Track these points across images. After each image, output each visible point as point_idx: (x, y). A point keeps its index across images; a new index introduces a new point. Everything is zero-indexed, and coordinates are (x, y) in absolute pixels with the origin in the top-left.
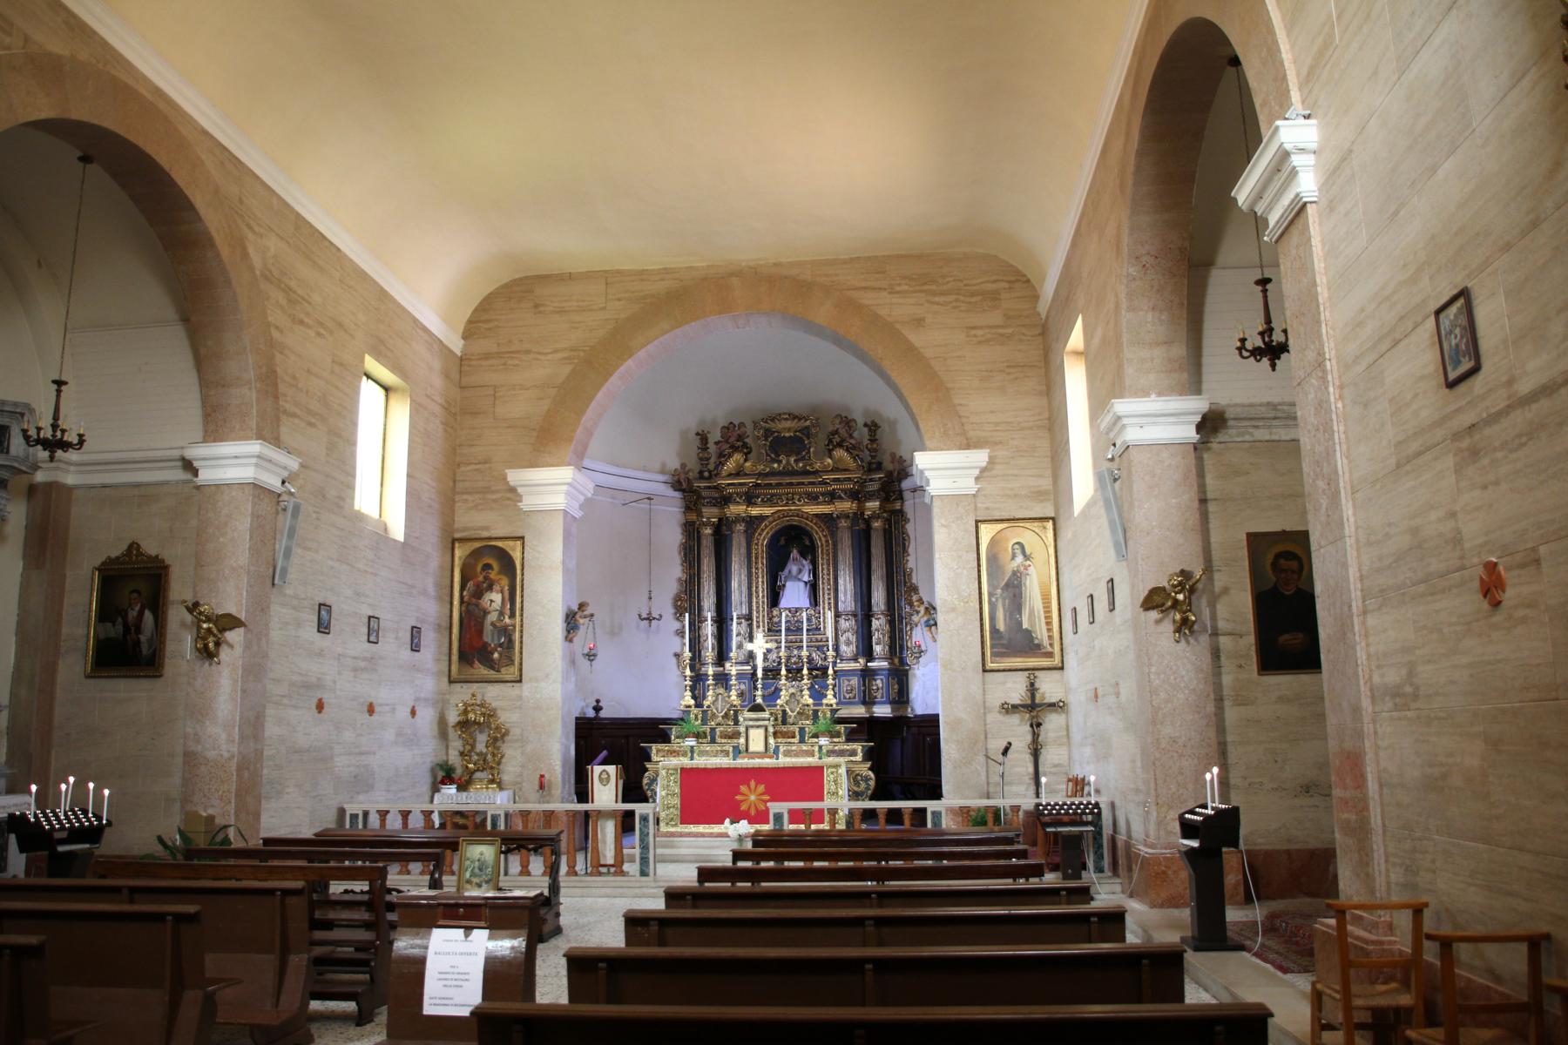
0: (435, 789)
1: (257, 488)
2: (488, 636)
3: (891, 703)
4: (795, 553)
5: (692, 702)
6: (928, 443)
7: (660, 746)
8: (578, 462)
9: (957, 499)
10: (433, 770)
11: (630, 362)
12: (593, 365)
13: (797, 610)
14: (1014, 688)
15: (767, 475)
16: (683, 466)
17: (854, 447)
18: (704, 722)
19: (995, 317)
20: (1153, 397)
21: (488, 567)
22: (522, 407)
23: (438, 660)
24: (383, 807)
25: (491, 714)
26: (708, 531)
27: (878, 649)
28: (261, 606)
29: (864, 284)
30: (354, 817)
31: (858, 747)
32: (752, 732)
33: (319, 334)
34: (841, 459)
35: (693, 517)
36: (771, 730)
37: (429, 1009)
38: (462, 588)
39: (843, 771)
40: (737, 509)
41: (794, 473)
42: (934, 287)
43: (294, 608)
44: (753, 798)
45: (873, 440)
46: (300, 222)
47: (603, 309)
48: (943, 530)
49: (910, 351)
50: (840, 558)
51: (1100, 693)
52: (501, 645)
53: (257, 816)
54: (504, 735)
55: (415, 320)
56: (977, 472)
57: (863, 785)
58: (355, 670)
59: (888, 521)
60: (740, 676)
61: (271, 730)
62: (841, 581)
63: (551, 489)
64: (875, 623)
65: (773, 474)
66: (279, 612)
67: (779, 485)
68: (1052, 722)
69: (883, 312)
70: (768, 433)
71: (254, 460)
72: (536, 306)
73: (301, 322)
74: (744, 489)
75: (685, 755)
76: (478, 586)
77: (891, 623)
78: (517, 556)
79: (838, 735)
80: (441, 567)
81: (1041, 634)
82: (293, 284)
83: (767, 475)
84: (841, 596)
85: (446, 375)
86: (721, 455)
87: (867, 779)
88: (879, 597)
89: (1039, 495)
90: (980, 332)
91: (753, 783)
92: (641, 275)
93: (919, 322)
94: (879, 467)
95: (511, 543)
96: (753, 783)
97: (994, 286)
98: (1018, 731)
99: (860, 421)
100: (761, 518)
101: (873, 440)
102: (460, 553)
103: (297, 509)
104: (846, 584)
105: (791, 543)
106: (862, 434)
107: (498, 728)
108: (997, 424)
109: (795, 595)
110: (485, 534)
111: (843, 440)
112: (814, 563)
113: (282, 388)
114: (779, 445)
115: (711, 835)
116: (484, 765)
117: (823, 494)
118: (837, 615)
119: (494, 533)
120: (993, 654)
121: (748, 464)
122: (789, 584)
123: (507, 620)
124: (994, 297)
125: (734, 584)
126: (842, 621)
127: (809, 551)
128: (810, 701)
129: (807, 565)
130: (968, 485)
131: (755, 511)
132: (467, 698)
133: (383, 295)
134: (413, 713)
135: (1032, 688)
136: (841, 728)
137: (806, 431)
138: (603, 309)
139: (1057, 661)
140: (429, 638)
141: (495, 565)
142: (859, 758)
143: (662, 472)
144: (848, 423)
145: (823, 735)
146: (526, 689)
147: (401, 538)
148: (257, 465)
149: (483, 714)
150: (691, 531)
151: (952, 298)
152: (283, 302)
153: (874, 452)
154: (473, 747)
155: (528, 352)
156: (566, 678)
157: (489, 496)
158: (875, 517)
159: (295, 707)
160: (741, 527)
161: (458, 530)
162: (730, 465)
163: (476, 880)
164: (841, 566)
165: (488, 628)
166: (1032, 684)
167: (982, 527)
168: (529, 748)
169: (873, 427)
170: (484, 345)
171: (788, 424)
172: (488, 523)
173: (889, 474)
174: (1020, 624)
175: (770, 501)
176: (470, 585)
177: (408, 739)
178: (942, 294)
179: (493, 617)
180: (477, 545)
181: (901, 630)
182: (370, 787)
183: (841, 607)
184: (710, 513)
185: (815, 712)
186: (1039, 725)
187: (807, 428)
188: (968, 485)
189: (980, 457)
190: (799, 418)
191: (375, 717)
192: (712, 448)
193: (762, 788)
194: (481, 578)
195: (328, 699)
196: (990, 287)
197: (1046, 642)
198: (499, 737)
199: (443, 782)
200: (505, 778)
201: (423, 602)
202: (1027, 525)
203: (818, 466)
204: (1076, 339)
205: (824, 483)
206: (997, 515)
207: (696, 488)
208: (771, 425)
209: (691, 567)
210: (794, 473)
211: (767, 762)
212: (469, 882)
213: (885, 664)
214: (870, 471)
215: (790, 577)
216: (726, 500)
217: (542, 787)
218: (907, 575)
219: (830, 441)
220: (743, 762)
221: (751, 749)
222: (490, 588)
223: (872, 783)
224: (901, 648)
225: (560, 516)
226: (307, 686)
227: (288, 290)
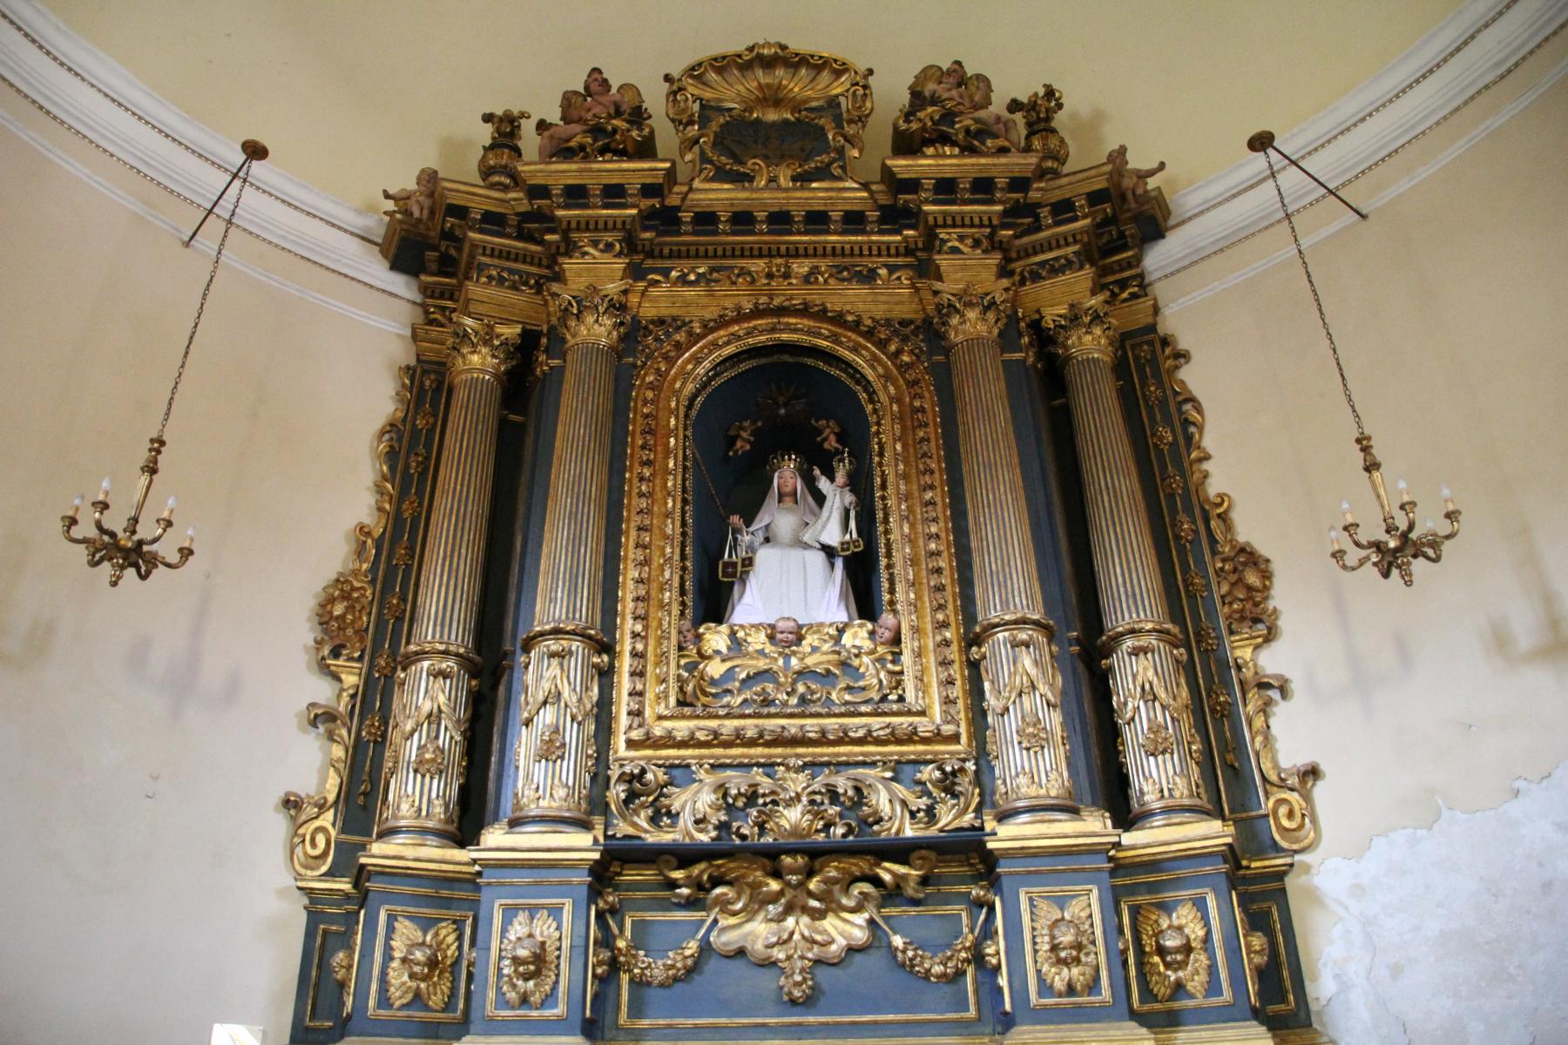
4: (786, 474)
109: (789, 581)
111: (949, 117)
112: (860, 484)
129: (837, 496)
150: (427, 386)
192: (530, 141)
218: (1212, 516)
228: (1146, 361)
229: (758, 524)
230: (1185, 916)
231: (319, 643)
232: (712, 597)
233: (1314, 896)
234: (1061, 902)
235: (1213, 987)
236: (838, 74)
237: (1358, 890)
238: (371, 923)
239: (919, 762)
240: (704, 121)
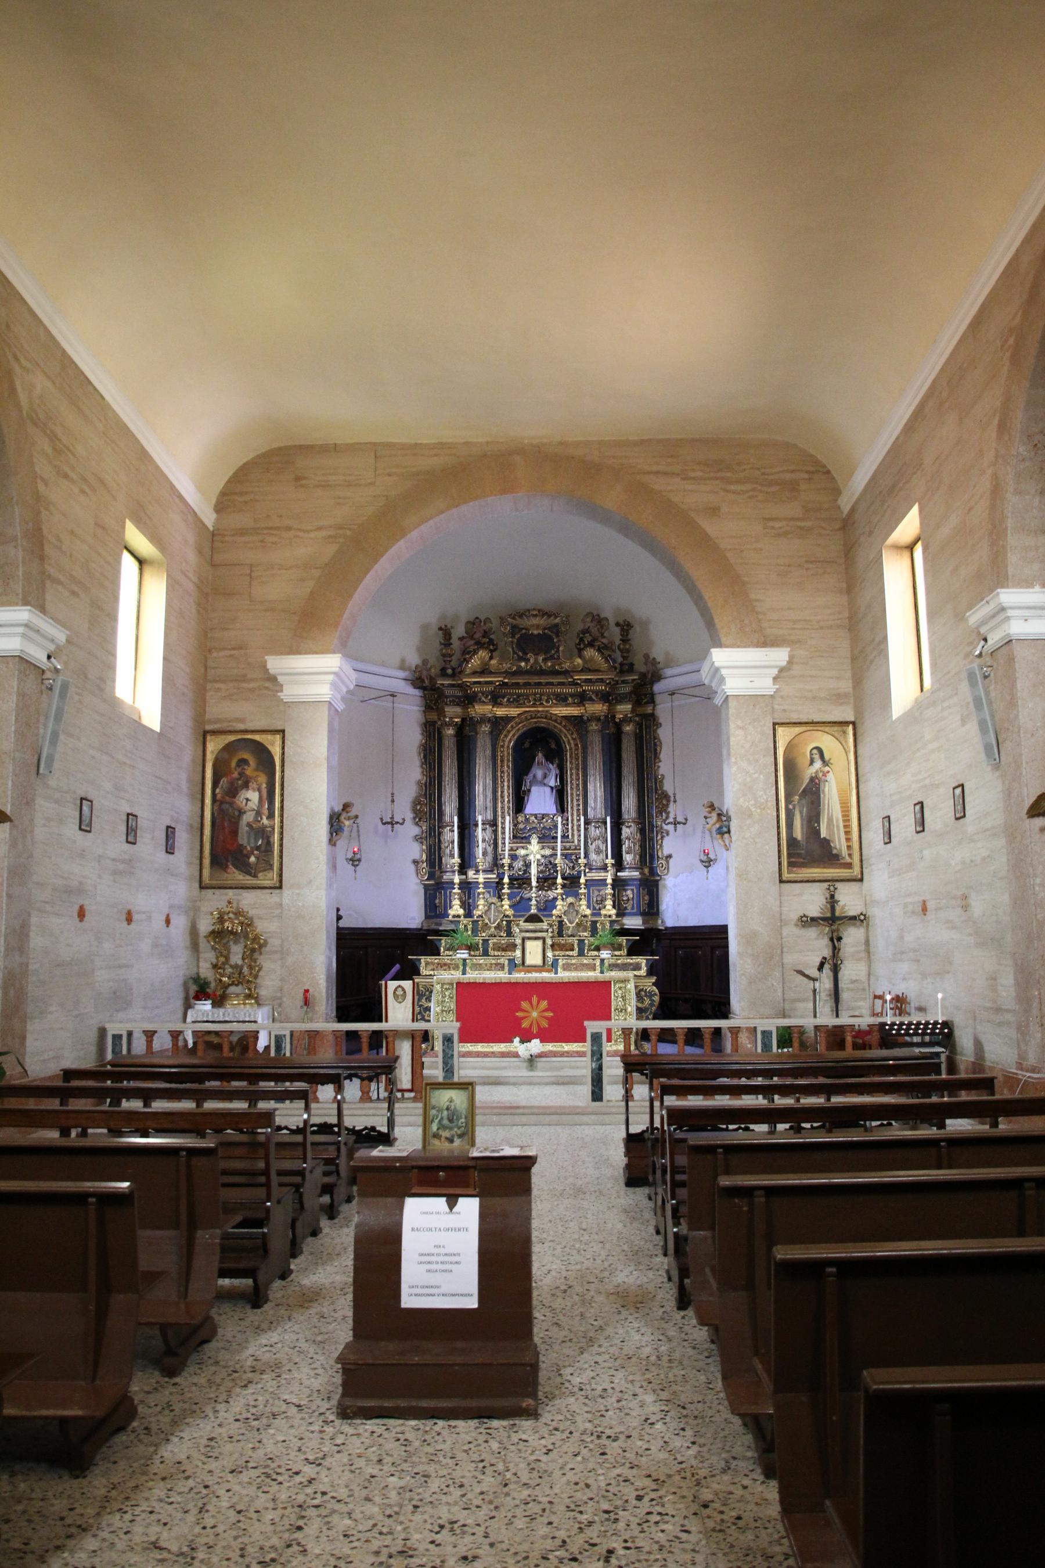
0: (188, 1006)
1: (23, 661)
2: (243, 838)
3: (643, 914)
5: (461, 912)
6: (723, 640)
7: (429, 959)
8: (344, 648)
9: (755, 699)
10: (185, 984)
11: (401, 544)
12: (361, 544)
13: (544, 816)
14: (811, 900)
15: (515, 674)
16: (425, 662)
17: (606, 647)
18: (475, 931)
19: (793, 509)
20: (1037, 588)
21: (243, 762)
22: (281, 588)
23: (189, 864)
24: (150, 1027)
25: (248, 924)
26: (451, 731)
27: (628, 858)
28: (26, 800)
29: (654, 468)
30: (117, 1038)
31: (642, 961)
32: (529, 944)
33: (83, 492)
34: (592, 659)
35: (434, 716)
36: (549, 942)
37: (409, 1301)
38: (215, 784)
39: (631, 986)
40: (482, 709)
41: (542, 672)
42: (729, 475)
43: (57, 802)
44: (535, 1014)
45: (625, 640)
46: (66, 362)
47: (373, 484)
48: (739, 732)
49: (705, 541)
50: (590, 762)
51: (930, 905)
52: (258, 848)
53: (23, 1038)
54: (261, 946)
55: (172, 487)
56: (775, 671)
57: (647, 1001)
58: (115, 873)
59: (640, 725)
60: (486, 884)
61: (36, 941)
62: (590, 787)
63: (315, 678)
64: (626, 832)
65: (519, 672)
66: (43, 807)
67: (527, 685)
68: (852, 937)
69: (676, 499)
70: (515, 629)
71: (21, 630)
72: (298, 479)
73: (66, 476)
74: (491, 688)
75: (456, 968)
76: (232, 783)
77: (642, 831)
78: (276, 751)
79: (619, 948)
80: (193, 761)
81: (840, 844)
82: (58, 431)
83: (515, 674)
84: (591, 802)
85: (200, 551)
86: (465, 652)
87: (650, 995)
88: (629, 804)
89: (838, 698)
90: (777, 525)
91: (535, 999)
92: (415, 449)
93: (713, 511)
94: (631, 669)
95: (270, 737)
96: (535, 999)
97: (793, 476)
98: (814, 947)
99: (612, 622)
100: (507, 719)
101: (625, 640)
102: (214, 746)
103: (65, 687)
104: (596, 790)
105: (538, 746)
106: (615, 634)
107: (256, 939)
108: (795, 622)
109: (540, 801)
110: (241, 726)
111: (594, 640)
112: (562, 769)
113: (48, 550)
114: (526, 643)
115: (486, 1055)
116: (239, 980)
117: (572, 696)
118: (587, 823)
119: (250, 726)
120: (791, 864)
121: (493, 662)
122: (534, 789)
123: (265, 821)
124: (792, 488)
125: (479, 788)
126: (591, 828)
127: (556, 755)
128: (588, 912)
129: (554, 770)
130: (765, 685)
131: (500, 712)
132: (222, 905)
133: (144, 456)
134: (168, 922)
135: (832, 901)
136: (623, 940)
137: (555, 629)
138: (373, 484)
139: (856, 871)
140: (182, 838)
141: (252, 762)
142: (643, 972)
143: (402, 667)
144: (600, 621)
145: (605, 947)
146: (287, 895)
147: (157, 728)
148: (24, 636)
149: (241, 924)
150: (432, 731)
151: (749, 486)
152: (49, 450)
153: (626, 652)
154: (227, 958)
155: (289, 528)
156: (330, 886)
157: (245, 685)
158: (626, 720)
159: (58, 915)
160: (486, 728)
161: (209, 722)
162: (475, 662)
163: (446, 1134)
164: (591, 771)
165: (243, 829)
166: (832, 896)
167: (780, 730)
168: (290, 960)
169: (626, 627)
170: (242, 520)
171: (535, 621)
172: (248, 715)
173: (643, 676)
174: (818, 832)
175: (516, 702)
176: (224, 782)
177: (164, 951)
178: (739, 482)
179: (248, 817)
180: (232, 738)
181: (651, 839)
182: (128, 1004)
183: (591, 814)
184: (453, 712)
185: (594, 923)
186: (840, 939)
187: (557, 625)
188: (765, 685)
189: (780, 656)
190: (548, 615)
191: (133, 926)
192: (456, 643)
193: (544, 1004)
194: (236, 775)
195: (90, 908)
196: (788, 476)
197: (844, 852)
198: (255, 947)
199: (197, 998)
200: (263, 992)
201: (172, 800)
202: (827, 729)
203: (567, 666)
204: (909, 525)
205: (574, 684)
206: (795, 718)
207: (438, 686)
208: (519, 621)
209: (431, 769)
210: (542, 672)
211: (546, 976)
212: (436, 1136)
213: (636, 874)
214: (622, 672)
215: (535, 781)
216: (469, 699)
217: (306, 1002)
218: (658, 782)
219: (582, 640)
220: (519, 976)
221: (529, 961)
222: (246, 786)
223: (657, 999)
224: (652, 857)
225: (326, 708)
226: (69, 891)
227: (53, 438)
228: (647, 724)
229: (531, 775)
230: (629, 892)
231: (414, 818)
232: (519, 805)
233: (665, 886)
234: (599, 891)
235: (633, 908)
236: (556, 617)
237: (675, 886)
238: (445, 894)
239: (572, 854)
240: (513, 634)
